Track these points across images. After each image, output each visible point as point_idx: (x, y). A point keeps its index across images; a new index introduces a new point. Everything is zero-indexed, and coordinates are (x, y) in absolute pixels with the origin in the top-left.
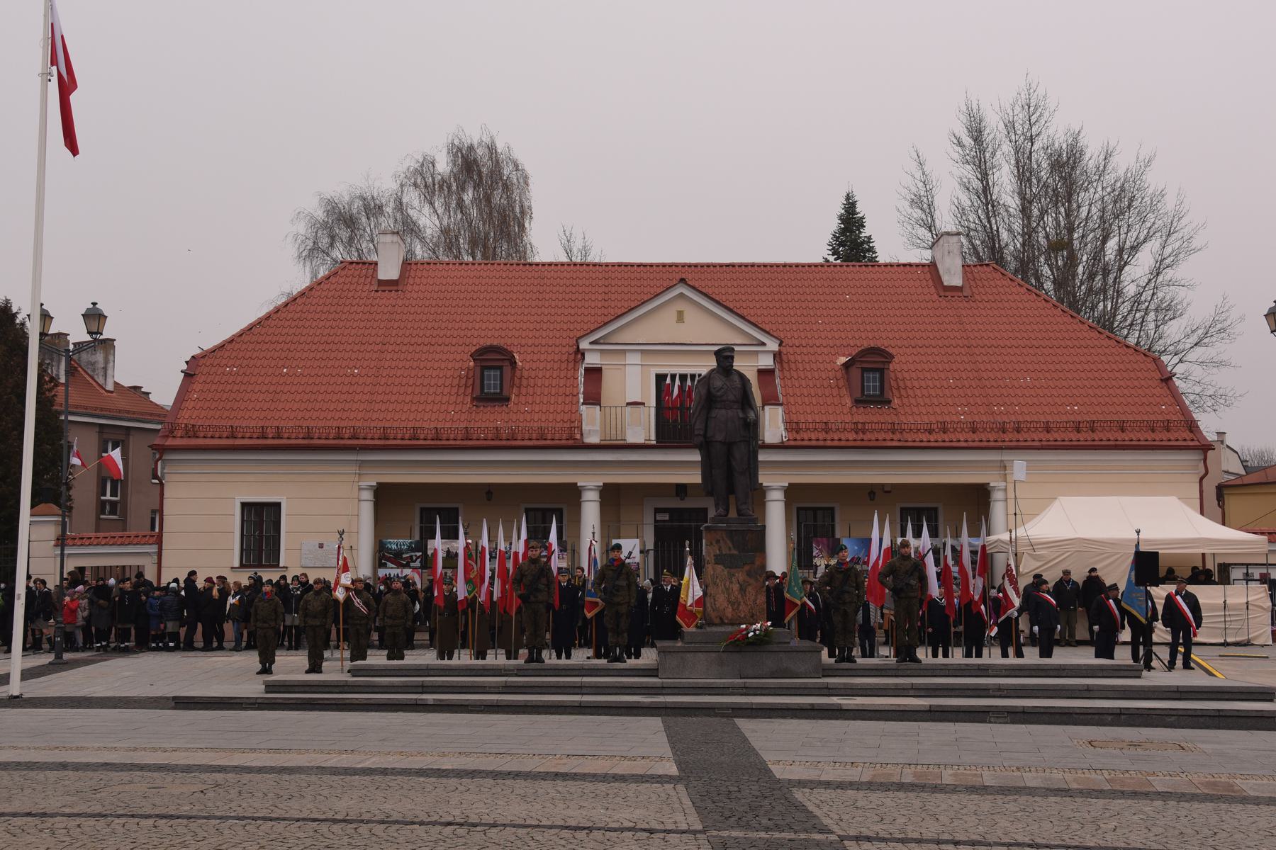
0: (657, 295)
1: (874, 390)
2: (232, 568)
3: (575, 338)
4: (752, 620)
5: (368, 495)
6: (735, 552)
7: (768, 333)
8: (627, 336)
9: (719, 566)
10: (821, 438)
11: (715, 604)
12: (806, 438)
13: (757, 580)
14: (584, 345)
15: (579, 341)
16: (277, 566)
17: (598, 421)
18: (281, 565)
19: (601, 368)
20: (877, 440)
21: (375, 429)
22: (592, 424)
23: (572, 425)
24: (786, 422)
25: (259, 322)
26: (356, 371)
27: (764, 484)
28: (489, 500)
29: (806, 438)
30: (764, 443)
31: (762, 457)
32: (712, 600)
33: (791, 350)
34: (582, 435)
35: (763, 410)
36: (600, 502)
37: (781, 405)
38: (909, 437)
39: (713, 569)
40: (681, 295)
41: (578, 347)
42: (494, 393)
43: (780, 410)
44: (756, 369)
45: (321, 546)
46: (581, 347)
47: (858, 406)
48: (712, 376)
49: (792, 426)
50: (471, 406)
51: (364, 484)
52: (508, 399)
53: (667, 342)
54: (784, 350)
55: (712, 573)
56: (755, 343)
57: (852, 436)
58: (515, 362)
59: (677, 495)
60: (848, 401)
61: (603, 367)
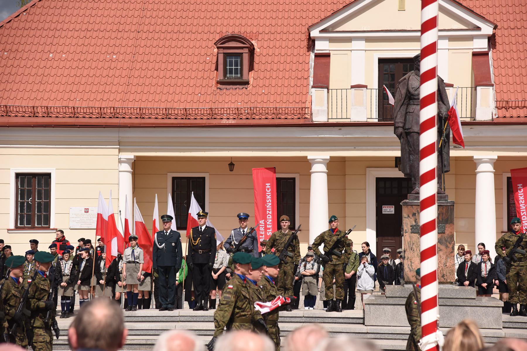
2: (8, 230)
3: (307, 26)
4: (442, 278)
5: (127, 167)
9: (415, 235)
11: (411, 266)
12: (515, 115)
13: (447, 247)
14: (314, 33)
15: (310, 30)
16: (48, 228)
18: (51, 227)
19: (330, 53)
21: (132, 109)
23: (303, 106)
26: (114, 57)
27: (475, 158)
28: (231, 171)
29: (515, 115)
30: (474, 120)
32: (409, 263)
33: (506, 33)
34: (312, 114)
35: (476, 90)
37: (492, 85)
39: (410, 237)
41: (310, 34)
44: (471, 52)
45: (87, 211)
46: (311, 36)
48: (410, 78)
50: (215, 89)
53: (389, 29)
54: (498, 32)
55: (409, 240)
56: (470, 28)
58: (254, 49)
59: (396, 166)
61: (332, 53)
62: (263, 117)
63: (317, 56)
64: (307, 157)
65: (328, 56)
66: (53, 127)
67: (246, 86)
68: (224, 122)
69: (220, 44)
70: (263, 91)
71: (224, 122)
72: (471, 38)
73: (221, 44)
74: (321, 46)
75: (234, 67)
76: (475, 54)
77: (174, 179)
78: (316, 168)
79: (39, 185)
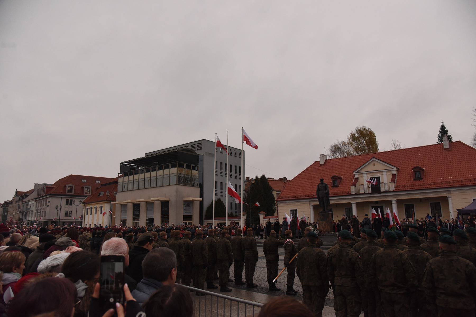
0: (368, 161)
5: (311, 207)
6: (323, 218)
7: (394, 166)
8: (363, 170)
9: (321, 221)
14: (354, 173)
17: (354, 190)
22: (353, 189)
25: (298, 175)
31: (330, 198)
40: (374, 160)
51: (311, 205)
52: (338, 186)
57: (411, 187)
58: (342, 178)
60: (412, 179)
61: (359, 177)
63: (355, 178)
76: (393, 175)
78: (353, 205)
79: (295, 212)
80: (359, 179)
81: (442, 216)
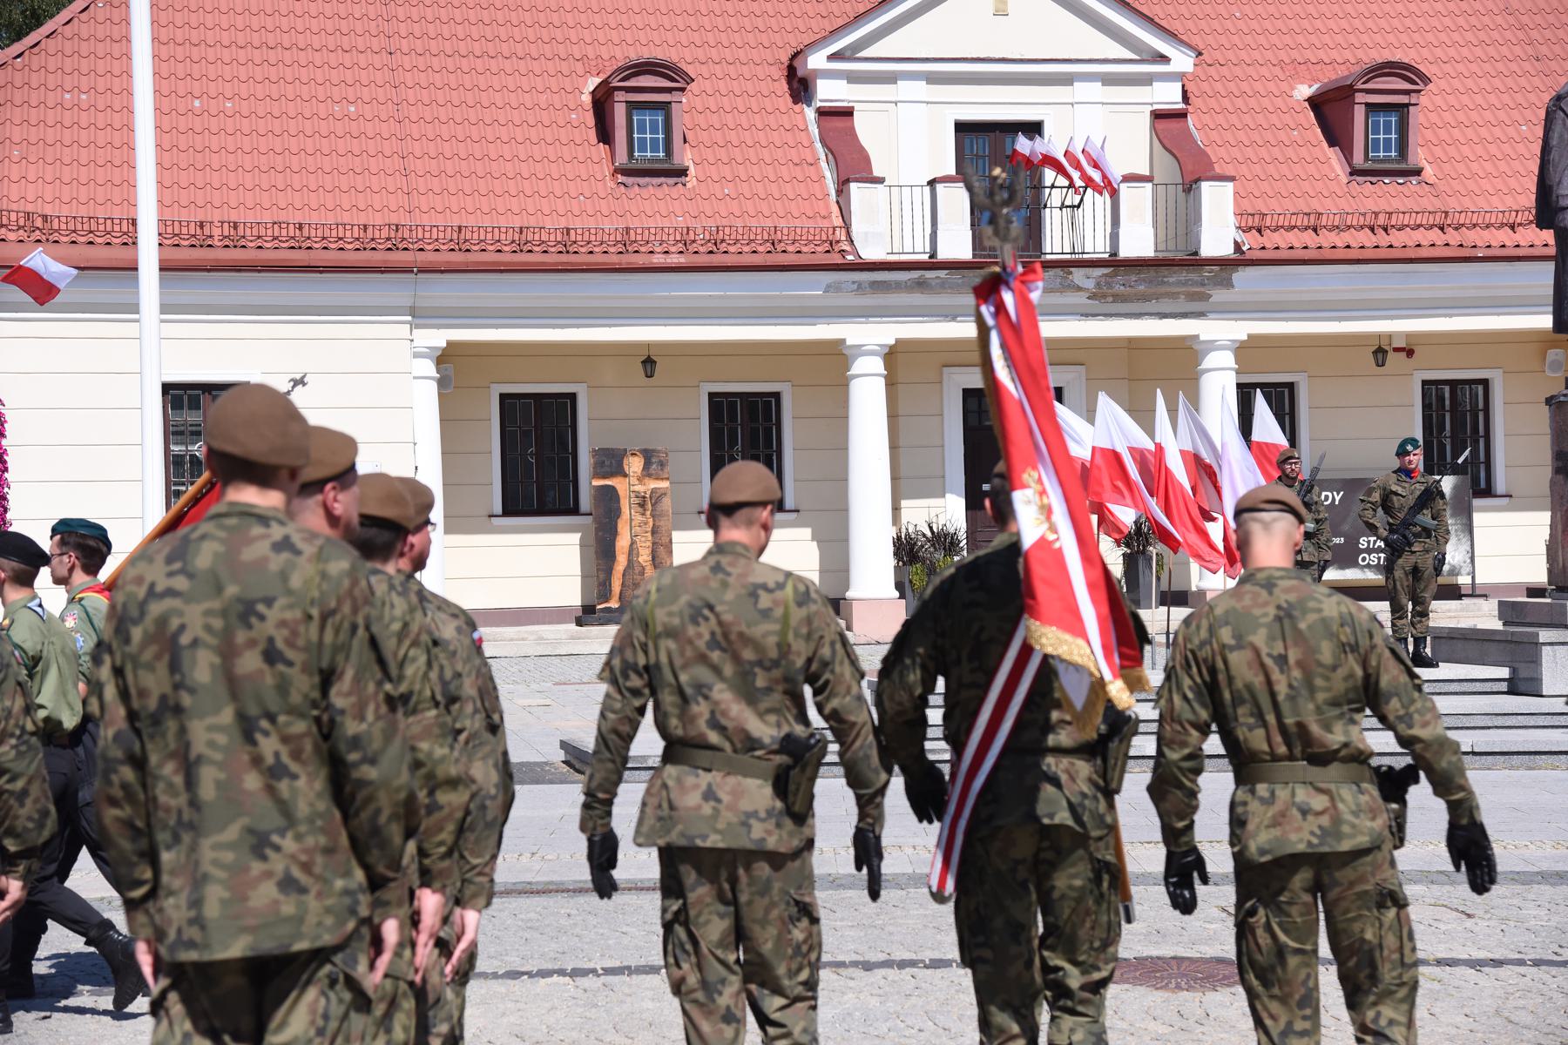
1: (1387, 149)
5: (429, 368)
10: (1311, 244)
14: (816, 61)
20: (1419, 245)
24: (1239, 214)
27: (1202, 338)
28: (651, 376)
36: (886, 377)
37: (1231, 179)
38: (1471, 237)
42: (651, 160)
43: (1229, 187)
47: (1360, 179)
49: (1252, 222)
50: (614, 186)
52: (683, 172)
57: (1365, 238)
61: (857, 106)
62: (746, 249)
64: (843, 341)
65: (848, 113)
66: (259, 271)
67: (683, 179)
68: (658, 259)
69: (619, 81)
70: (726, 191)
71: (675, 261)
72: (1146, 80)
73: (622, 80)
74: (829, 92)
75: (648, 136)
76: (1158, 116)
77: (503, 397)
78: (860, 366)
80: (858, 117)
81: (1500, 485)
